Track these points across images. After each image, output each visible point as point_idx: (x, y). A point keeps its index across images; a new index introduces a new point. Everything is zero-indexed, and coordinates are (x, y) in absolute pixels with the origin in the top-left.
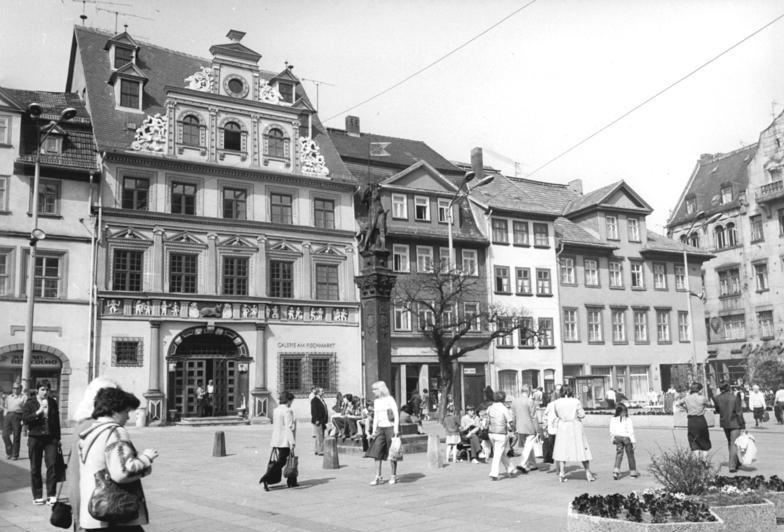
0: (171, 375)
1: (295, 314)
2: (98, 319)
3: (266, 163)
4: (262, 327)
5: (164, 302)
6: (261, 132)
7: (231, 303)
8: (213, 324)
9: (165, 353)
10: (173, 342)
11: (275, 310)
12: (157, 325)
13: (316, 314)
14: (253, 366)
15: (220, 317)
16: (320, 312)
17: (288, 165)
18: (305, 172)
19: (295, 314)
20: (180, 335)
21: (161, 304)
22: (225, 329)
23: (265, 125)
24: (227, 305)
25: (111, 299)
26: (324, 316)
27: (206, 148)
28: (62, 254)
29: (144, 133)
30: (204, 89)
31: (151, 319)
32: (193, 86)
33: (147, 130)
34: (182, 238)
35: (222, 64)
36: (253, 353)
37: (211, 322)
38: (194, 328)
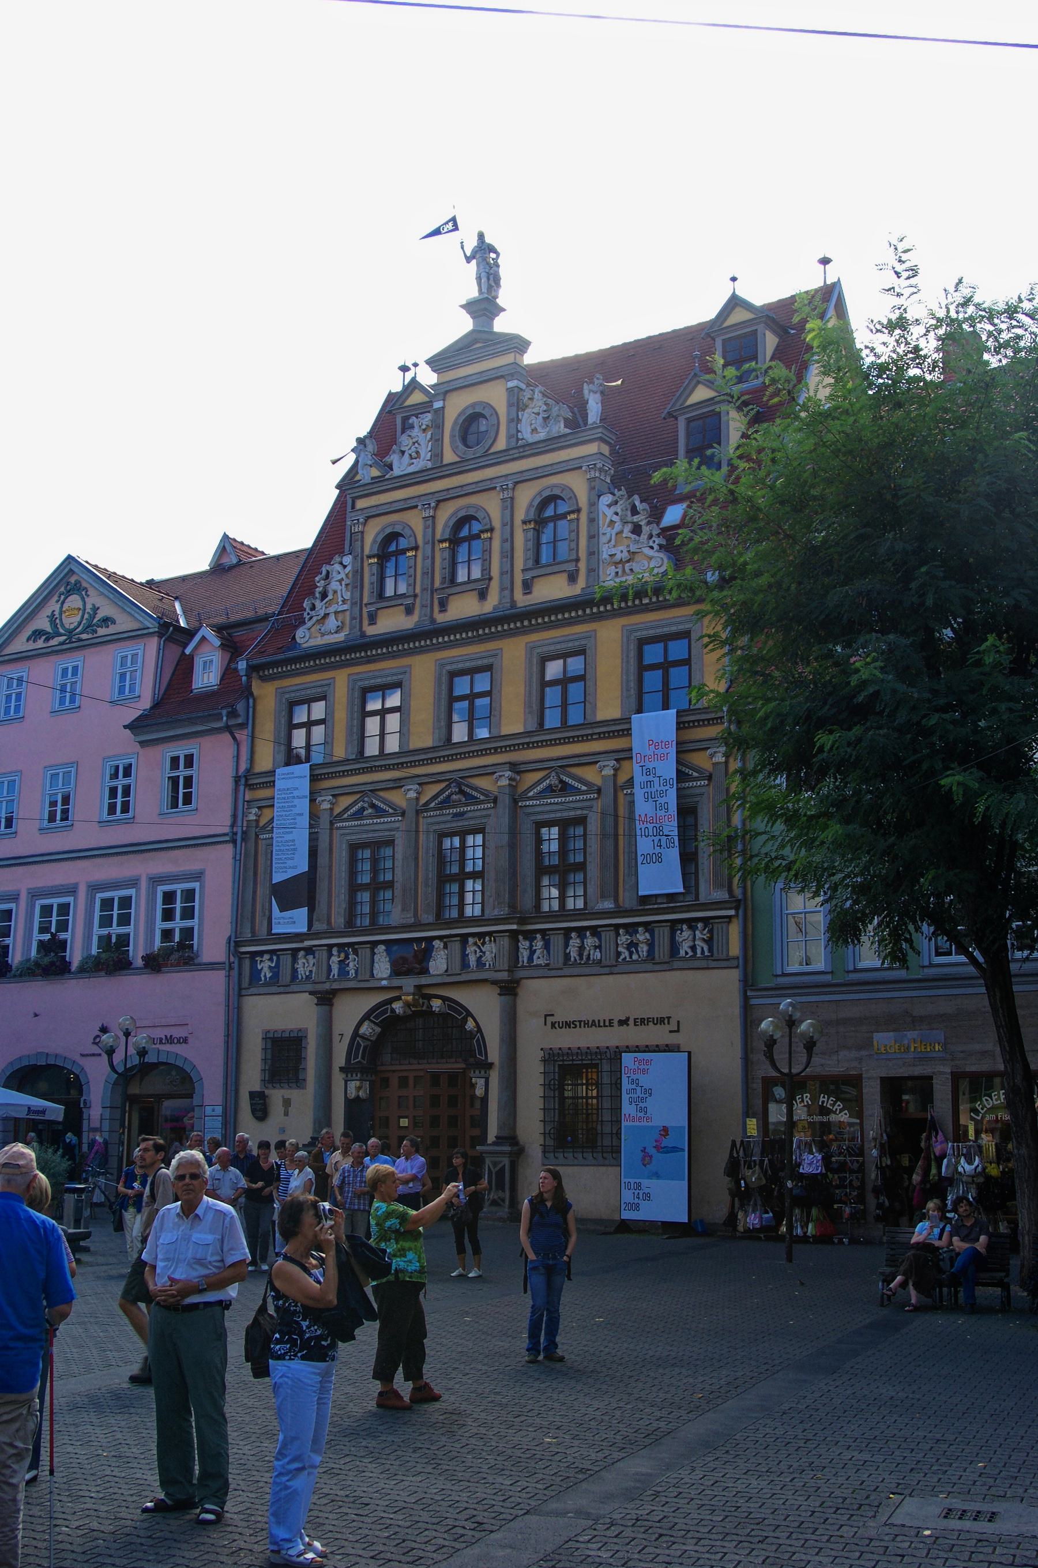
0: (352, 1104)
1: (581, 948)
2: (240, 996)
3: (527, 586)
4: (509, 989)
5: (335, 951)
6: (520, 515)
7: (440, 938)
8: (412, 990)
9: (340, 1059)
10: (356, 1034)
11: (539, 944)
12: (326, 999)
13: (632, 946)
14: (494, 1076)
15: (425, 971)
16: (642, 936)
17: (573, 578)
18: (609, 579)
19: (581, 948)
20: (366, 1017)
21: (330, 955)
22: (444, 999)
23: (526, 497)
24: (437, 943)
25: (261, 953)
26: (651, 945)
27: (415, 596)
28: (198, 876)
29: (318, 604)
30: (419, 465)
31: (310, 987)
32: (400, 466)
33: (324, 595)
34: (363, 809)
35: (446, 392)
36: (494, 1053)
37: (409, 983)
38: (390, 1001)
